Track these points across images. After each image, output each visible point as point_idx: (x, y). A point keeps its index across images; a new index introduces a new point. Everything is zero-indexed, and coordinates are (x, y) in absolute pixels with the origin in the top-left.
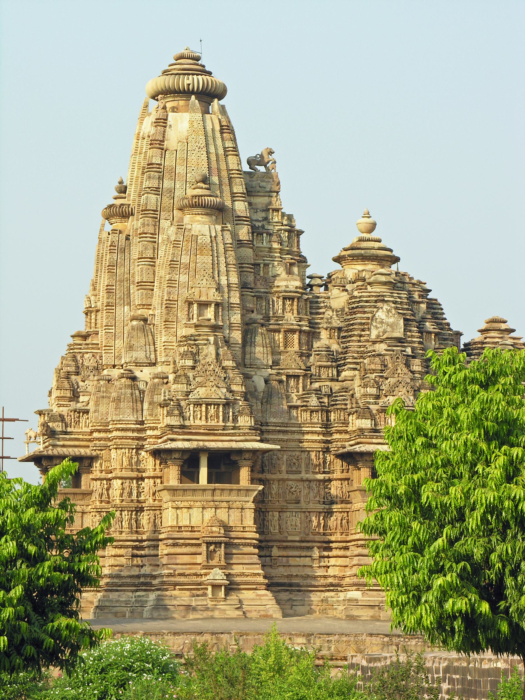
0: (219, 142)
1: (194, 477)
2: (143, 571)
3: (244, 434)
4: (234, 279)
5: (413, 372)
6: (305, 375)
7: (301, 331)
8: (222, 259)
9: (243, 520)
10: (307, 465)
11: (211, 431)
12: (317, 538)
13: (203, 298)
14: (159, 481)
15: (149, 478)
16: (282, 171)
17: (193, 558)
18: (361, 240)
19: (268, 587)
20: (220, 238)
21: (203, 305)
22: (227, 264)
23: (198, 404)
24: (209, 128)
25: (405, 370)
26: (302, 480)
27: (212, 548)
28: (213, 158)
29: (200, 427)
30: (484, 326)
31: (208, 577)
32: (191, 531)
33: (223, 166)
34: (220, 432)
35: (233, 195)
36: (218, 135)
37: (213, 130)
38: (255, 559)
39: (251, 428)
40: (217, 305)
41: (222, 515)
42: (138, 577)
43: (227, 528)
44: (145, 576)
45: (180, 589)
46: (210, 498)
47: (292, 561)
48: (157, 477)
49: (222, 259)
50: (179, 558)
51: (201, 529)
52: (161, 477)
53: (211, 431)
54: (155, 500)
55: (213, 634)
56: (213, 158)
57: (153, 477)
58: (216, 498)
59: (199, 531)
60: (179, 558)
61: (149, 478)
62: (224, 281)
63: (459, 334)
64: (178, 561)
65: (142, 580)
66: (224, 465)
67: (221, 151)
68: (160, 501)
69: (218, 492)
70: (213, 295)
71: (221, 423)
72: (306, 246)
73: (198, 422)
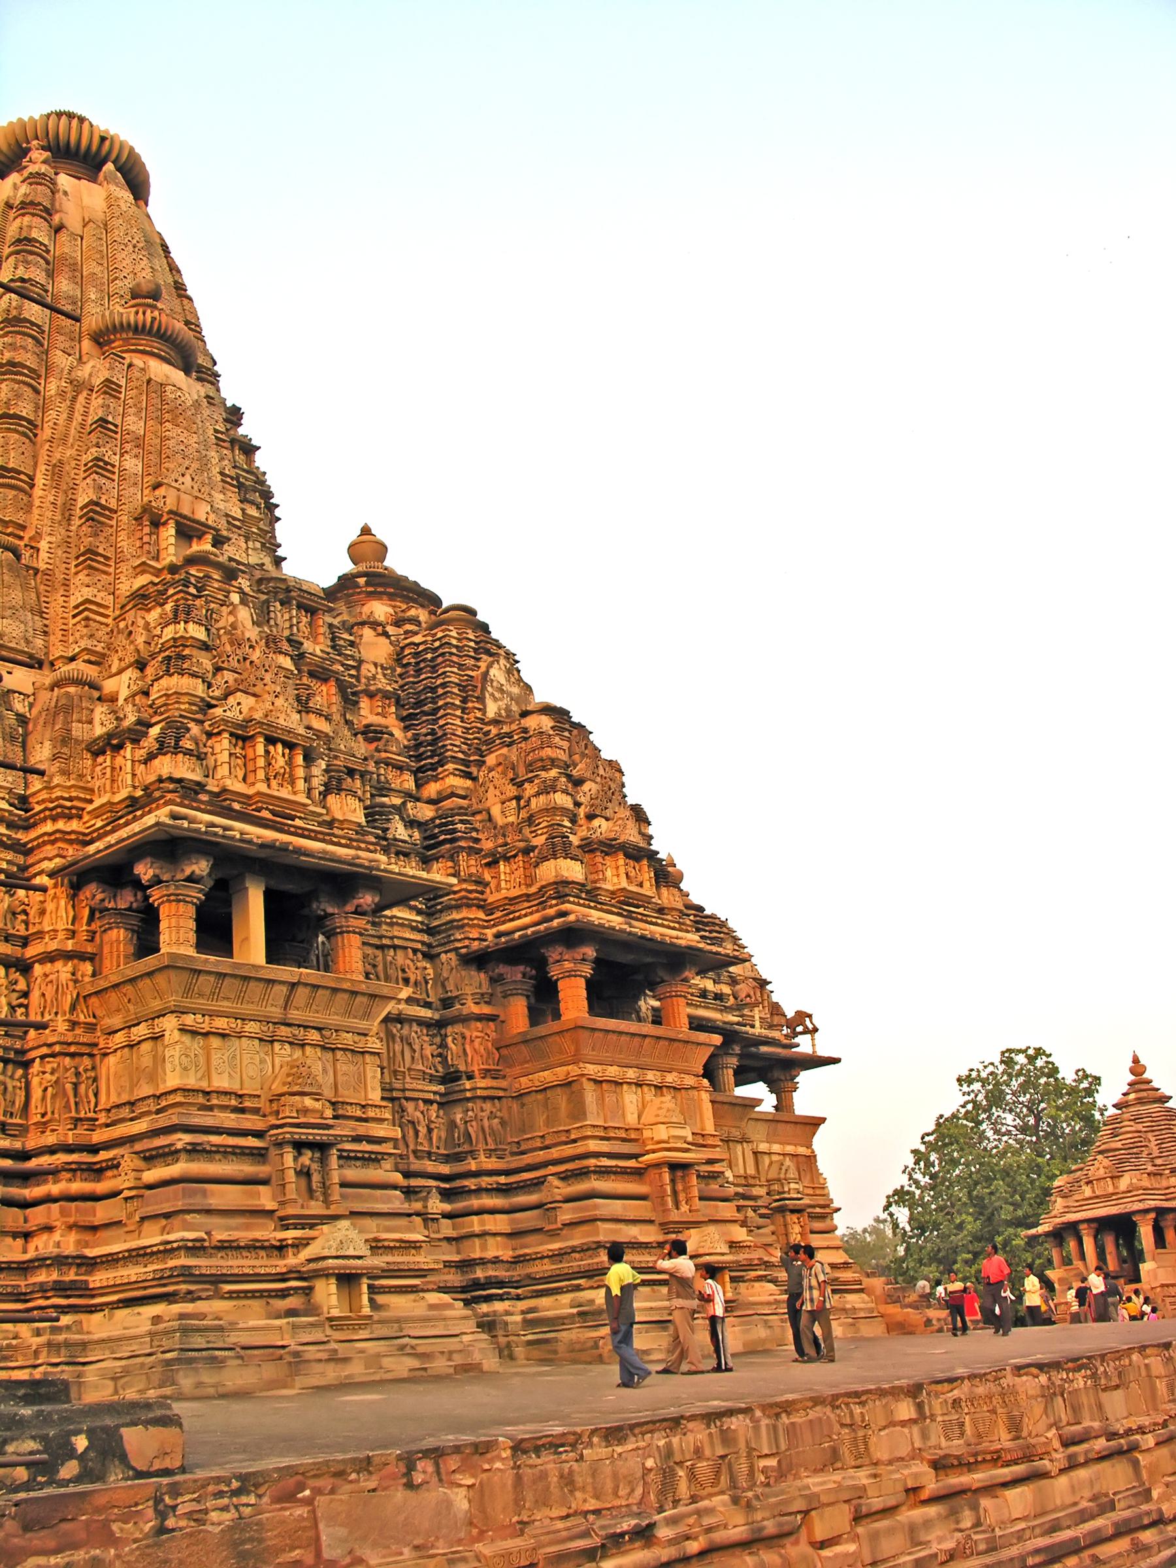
2: (42, 1245)
14: (88, 968)
15: (49, 958)
17: (252, 1195)
31: (305, 1254)
32: (236, 1110)
34: (298, 822)
42: (24, 1268)
44: (60, 1261)
45: (232, 1295)
46: (276, 1012)
48: (82, 957)
50: (213, 1194)
51: (261, 1104)
52: (91, 958)
54: (74, 1024)
55: (710, 1417)
57: (67, 956)
58: (295, 1015)
59: (256, 1111)
60: (213, 1194)
61: (49, 958)
64: (214, 1202)
65: (42, 1277)
68: (91, 1028)
69: (302, 993)
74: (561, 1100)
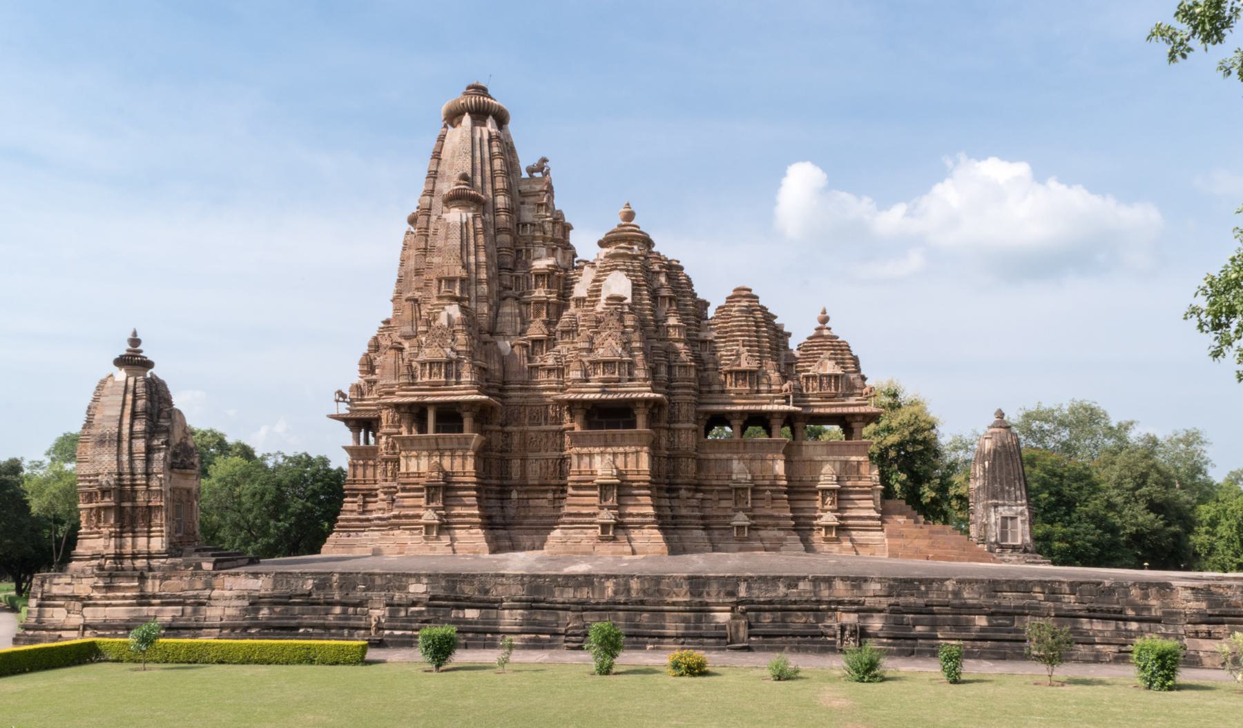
0: (486, 148)
1: (423, 428)
3: (465, 389)
4: (482, 258)
5: (625, 327)
6: (549, 340)
7: (549, 303)
8: (472, 242)
9: (464, 467)
10: (546, 419)
11: (435, 386)
12: (553, 482)
13: (452, 275)
16: (556, 177)
18: (620, 226)
19: (483, 526)
20: (471, 222)
21: (451, 281)
22: (476, 246)
23: (423, 364)
24: (478, 136)
25: (617, 324)
26: (540, 431)
27: (432, 491)
28: (478, 161)
29: (423, 384)
30: (731, 293)
33: (488, 168)
35: (494, 191)
36: (486, 143)
37: (481, 140)
38: (473, 500)
39: (471, 382)
40: (462, 280)
41: (446, 463)
43: (447, 475)
47: (531, 502)
49: (472, 242)
53: (435, 386)
56: (478, 161)
62: (472, 259)
63: (706, 304)
66: (449, 416)
67: (487, 155)
70: (459, 272)
71: (443, 379)
72: (574, 238)
73: (426, 379)
74: (586, 460)
